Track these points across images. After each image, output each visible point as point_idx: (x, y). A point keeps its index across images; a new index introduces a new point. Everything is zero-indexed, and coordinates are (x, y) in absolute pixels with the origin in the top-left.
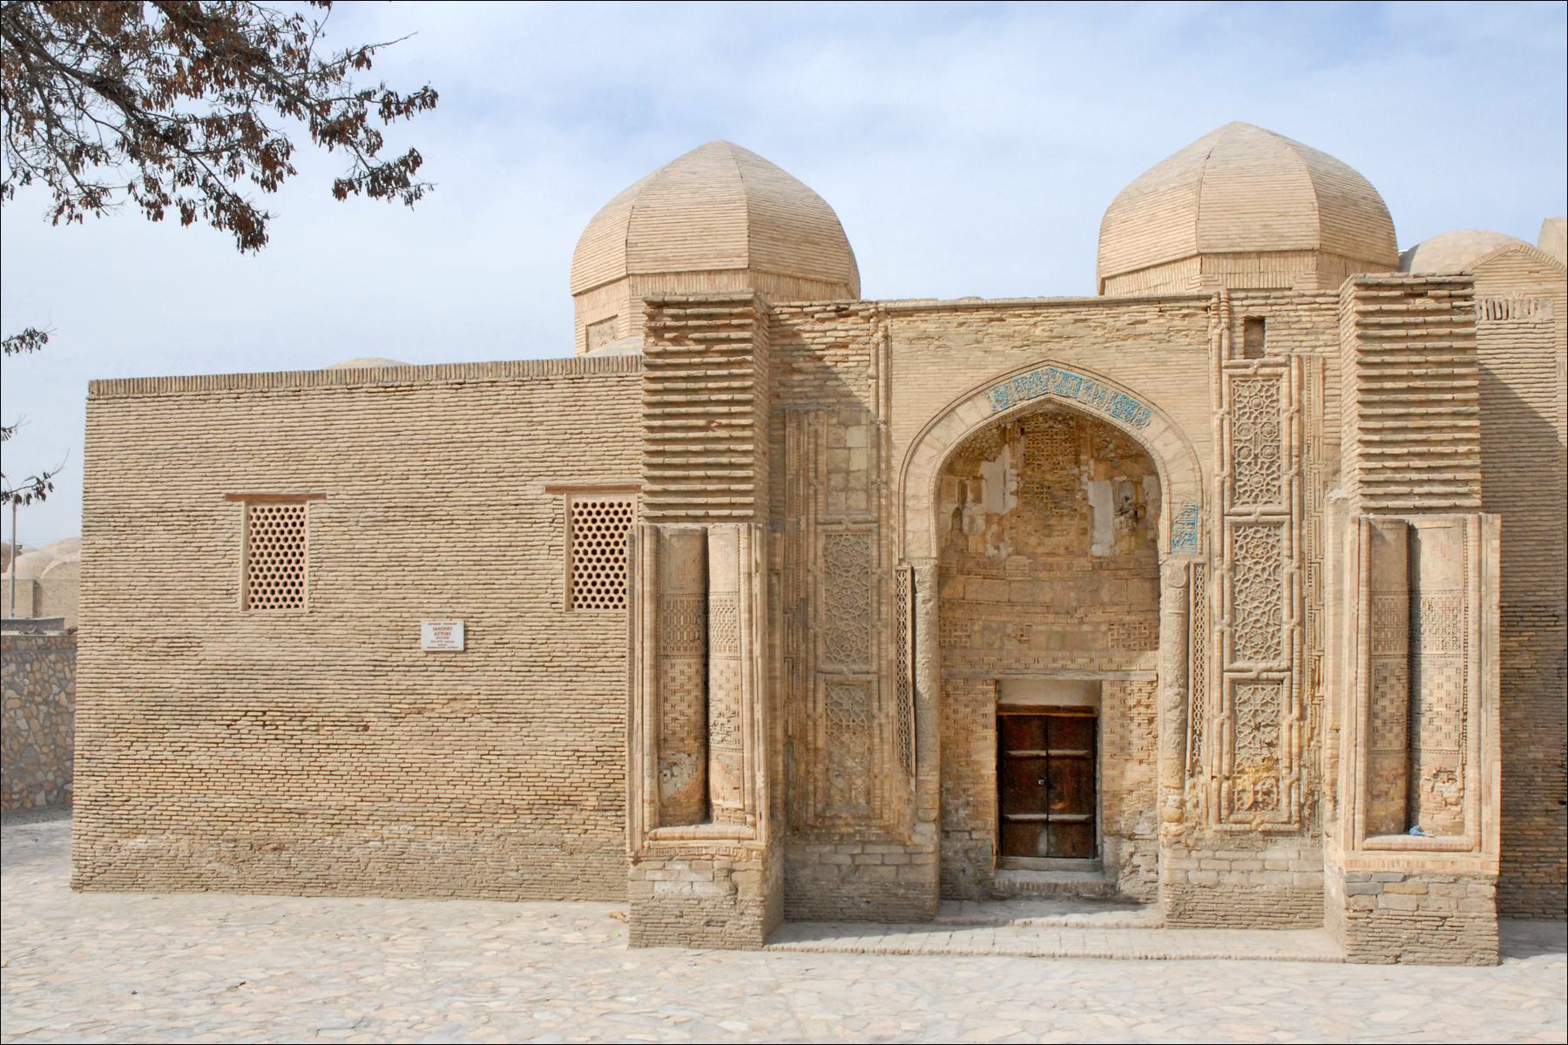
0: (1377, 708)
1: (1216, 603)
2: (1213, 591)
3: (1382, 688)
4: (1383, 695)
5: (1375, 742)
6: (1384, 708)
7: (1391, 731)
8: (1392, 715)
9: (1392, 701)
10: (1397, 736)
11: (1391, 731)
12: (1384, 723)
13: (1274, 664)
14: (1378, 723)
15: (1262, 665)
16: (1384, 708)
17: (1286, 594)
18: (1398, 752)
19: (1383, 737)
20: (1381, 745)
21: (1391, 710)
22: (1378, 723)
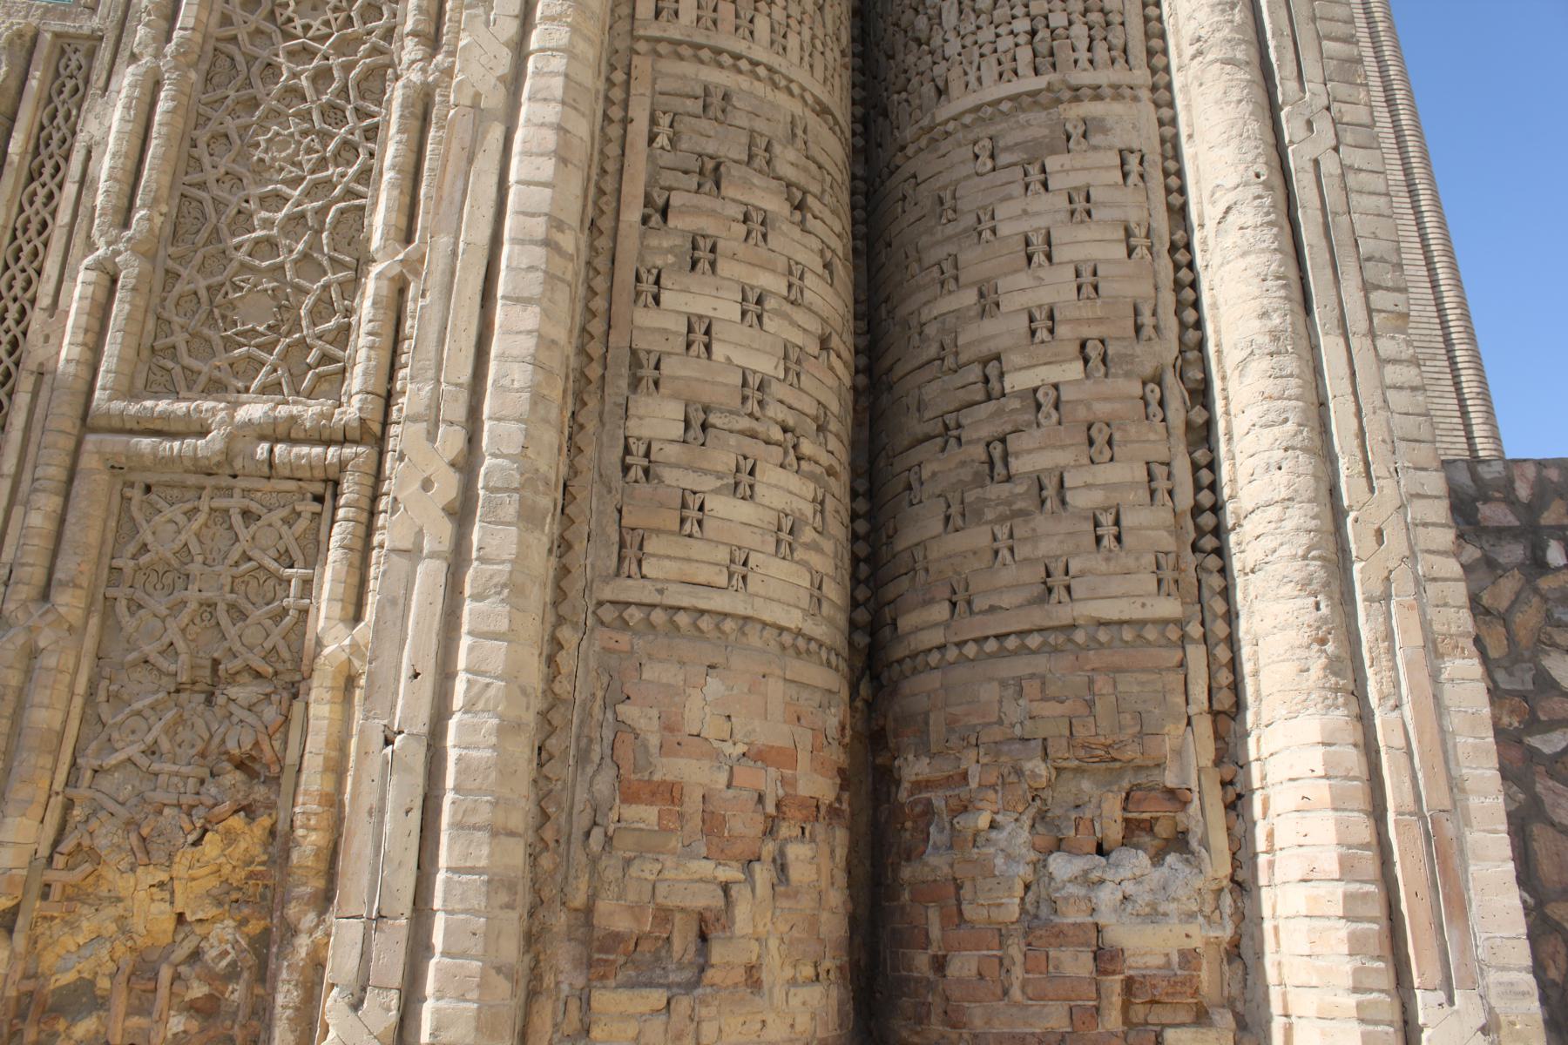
0: (656, 326)
1: (104, 166)
2: (108, 124)
3: (694, 214)
4: (700, 256)
5: (629, 549)
6: (700, 334)
7: (742, 483)
8: (754, 389)
9: (754, 305)
10: (786, 534)
11: (742, 483)
12: (699, 425)
13: (309, 411)
14: (659, 419)
15: (254, 410)
16: (700, 334)
17: (392, 149)
18: (796, 644)
19: (690, 514)
20: (672, 567)
21: (745, 352)
22: (659, 419)
